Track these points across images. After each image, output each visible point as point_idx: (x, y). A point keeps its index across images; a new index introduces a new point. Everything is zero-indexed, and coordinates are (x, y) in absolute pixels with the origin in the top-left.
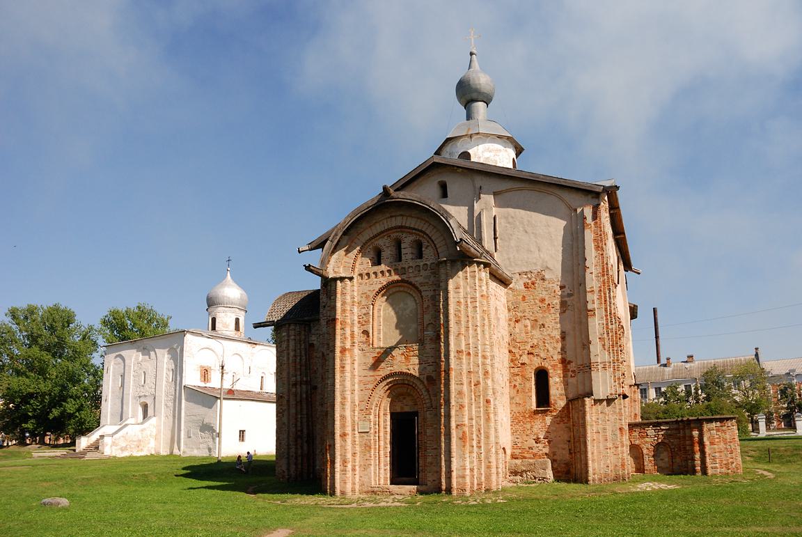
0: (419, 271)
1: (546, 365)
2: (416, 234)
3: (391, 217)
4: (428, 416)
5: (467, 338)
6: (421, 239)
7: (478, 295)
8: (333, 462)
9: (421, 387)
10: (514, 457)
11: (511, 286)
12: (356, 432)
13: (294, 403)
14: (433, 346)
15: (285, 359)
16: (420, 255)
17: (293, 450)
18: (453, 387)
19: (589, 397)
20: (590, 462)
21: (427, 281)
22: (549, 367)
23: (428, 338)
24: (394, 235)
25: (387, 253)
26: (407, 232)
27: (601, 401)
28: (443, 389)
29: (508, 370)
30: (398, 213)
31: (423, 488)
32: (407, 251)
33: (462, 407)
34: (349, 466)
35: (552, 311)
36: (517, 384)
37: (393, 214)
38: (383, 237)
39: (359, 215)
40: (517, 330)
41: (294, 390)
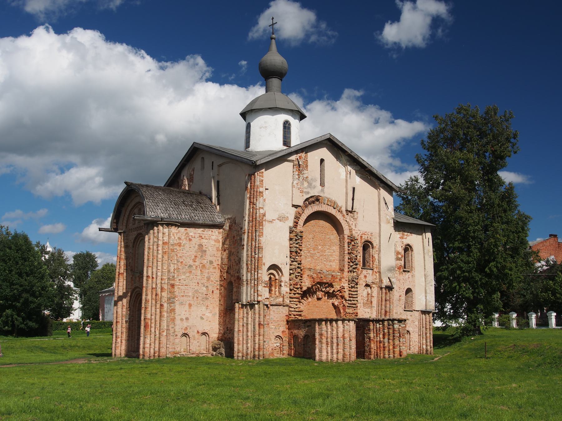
1: (233, 279)
3: (136, 196)
5: (152, 268)
7: (160, 243)
10: (219, 339)
11: (224, 227)
12: (124, 321)
18: (144, 297)
19: (238, 303)
20: (236, 345)
22: (233, 282)
24: (139, 206)
27: (246, 305)
29: (219, 283)
33: (146, 308)
34: (119, 340)
35: (237, 245)
36: (222, 292)
38: (136, 207)
40: (224, 256)
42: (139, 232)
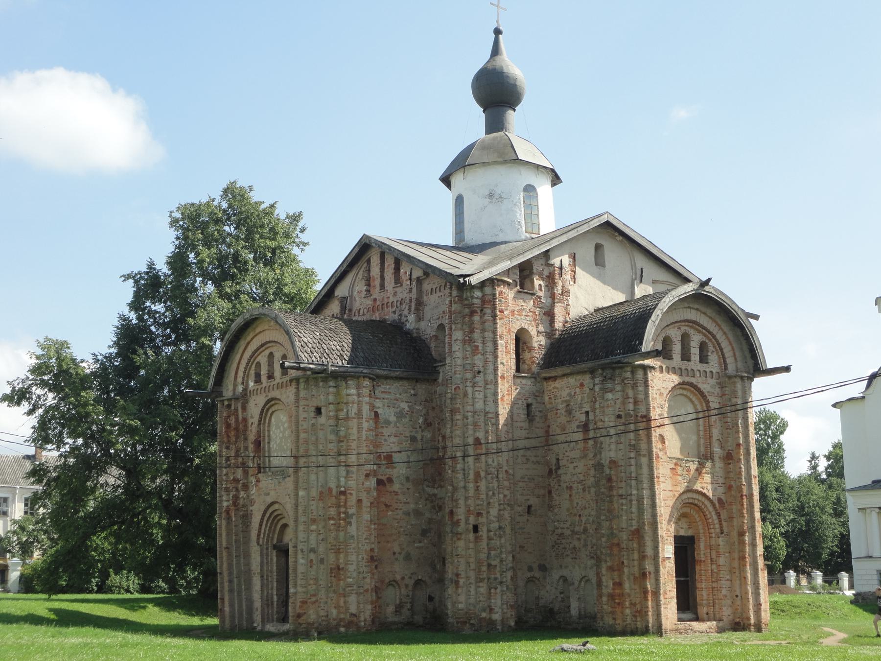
0: (706, 377)
2: (705, 335)
3: (689, 307)
4: (721, 543)
6: (707, 341)
8: (656, 594)
9: (711, 509)
13: (369, 504)
14: (722, 465)
15: (355, 431)
16: (703, 359)
17: (368, 580)
21: (713, 391)
23: (717, 455)
25: (677, 348)
26: (697, 330)
28: (746, 515)
30: (696, 306)
31: (721, 624)
32: (695, 352)
37: (691, 306)
38: (674, 328)
39: (677, 299)
41: (367, 484)
42: (687, 379)
